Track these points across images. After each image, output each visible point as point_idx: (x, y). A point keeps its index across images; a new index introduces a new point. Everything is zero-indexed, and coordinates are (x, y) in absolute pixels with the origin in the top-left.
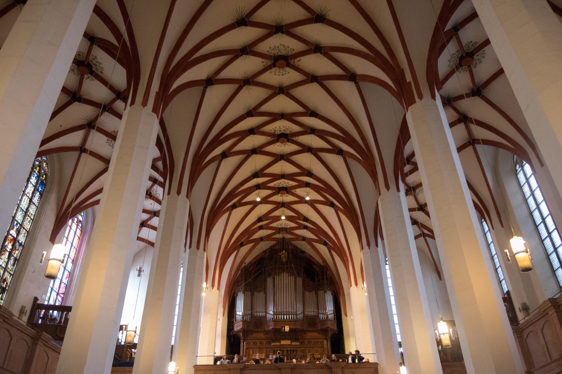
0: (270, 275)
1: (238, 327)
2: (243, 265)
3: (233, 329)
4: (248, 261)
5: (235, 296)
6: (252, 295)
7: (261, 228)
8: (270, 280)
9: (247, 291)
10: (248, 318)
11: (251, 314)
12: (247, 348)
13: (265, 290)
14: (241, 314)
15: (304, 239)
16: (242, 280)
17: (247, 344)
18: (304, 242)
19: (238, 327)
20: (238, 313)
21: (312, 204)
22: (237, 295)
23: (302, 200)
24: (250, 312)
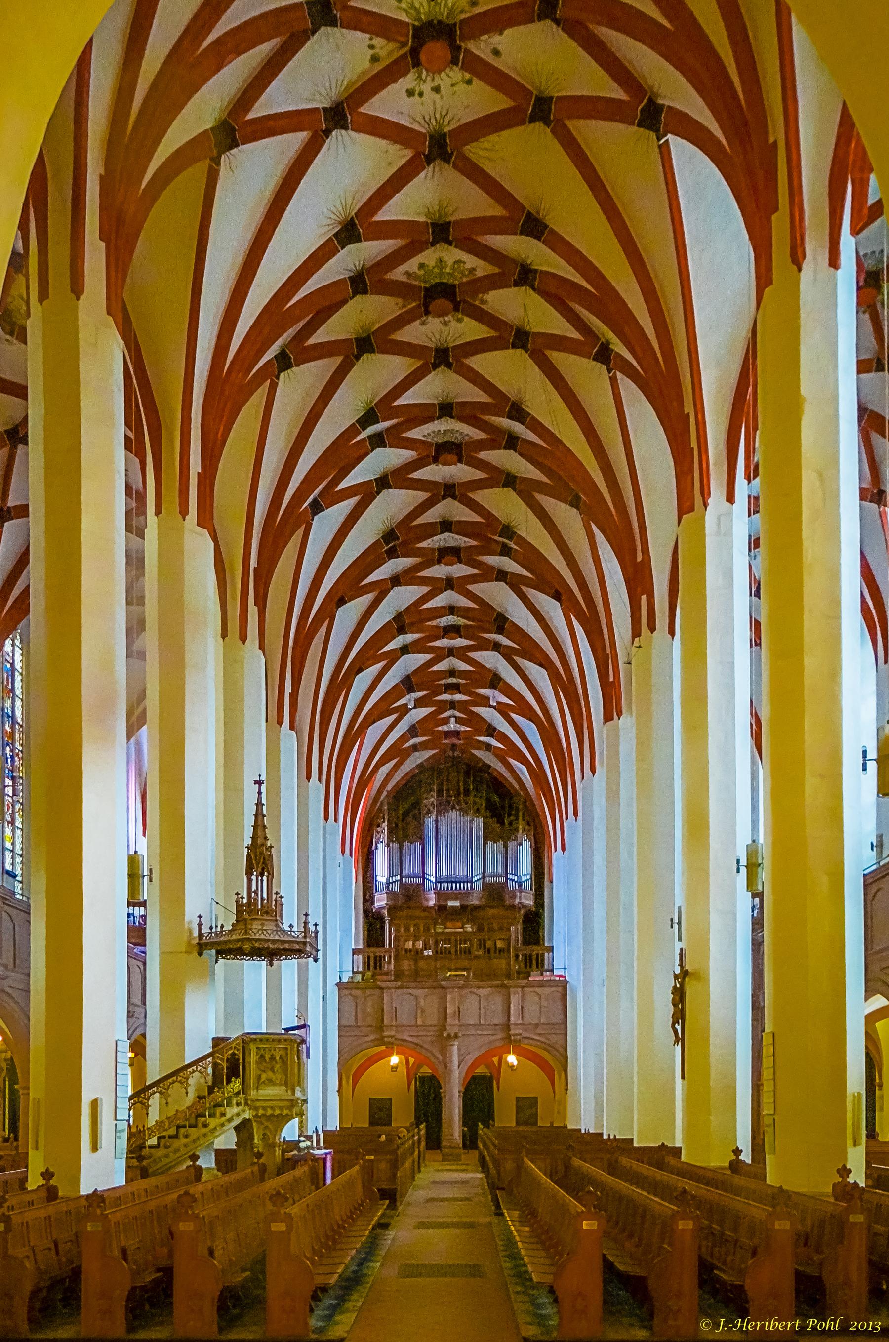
0: (429, 812)
1: (381, 901)
2: (385, 794)
3: (372, 903)
4: (389, 787)
5: (373, 848)
6: (401, 847)
7: (415, 748)
8: (429, 822)
9: (393, 842)
10: (397, 888)
11: (401, 880)
12: (395, 937)
13: (421, 838)
14: (384, 880)
15: (488, 747)
16: (384, 822)
17: (395, 931)
18: (488, 753)
19: (381, 901)
20: (379, 878)
21: (502, 709)
22: (376, 848)
23: (485, 701)
24: (398, 877)
